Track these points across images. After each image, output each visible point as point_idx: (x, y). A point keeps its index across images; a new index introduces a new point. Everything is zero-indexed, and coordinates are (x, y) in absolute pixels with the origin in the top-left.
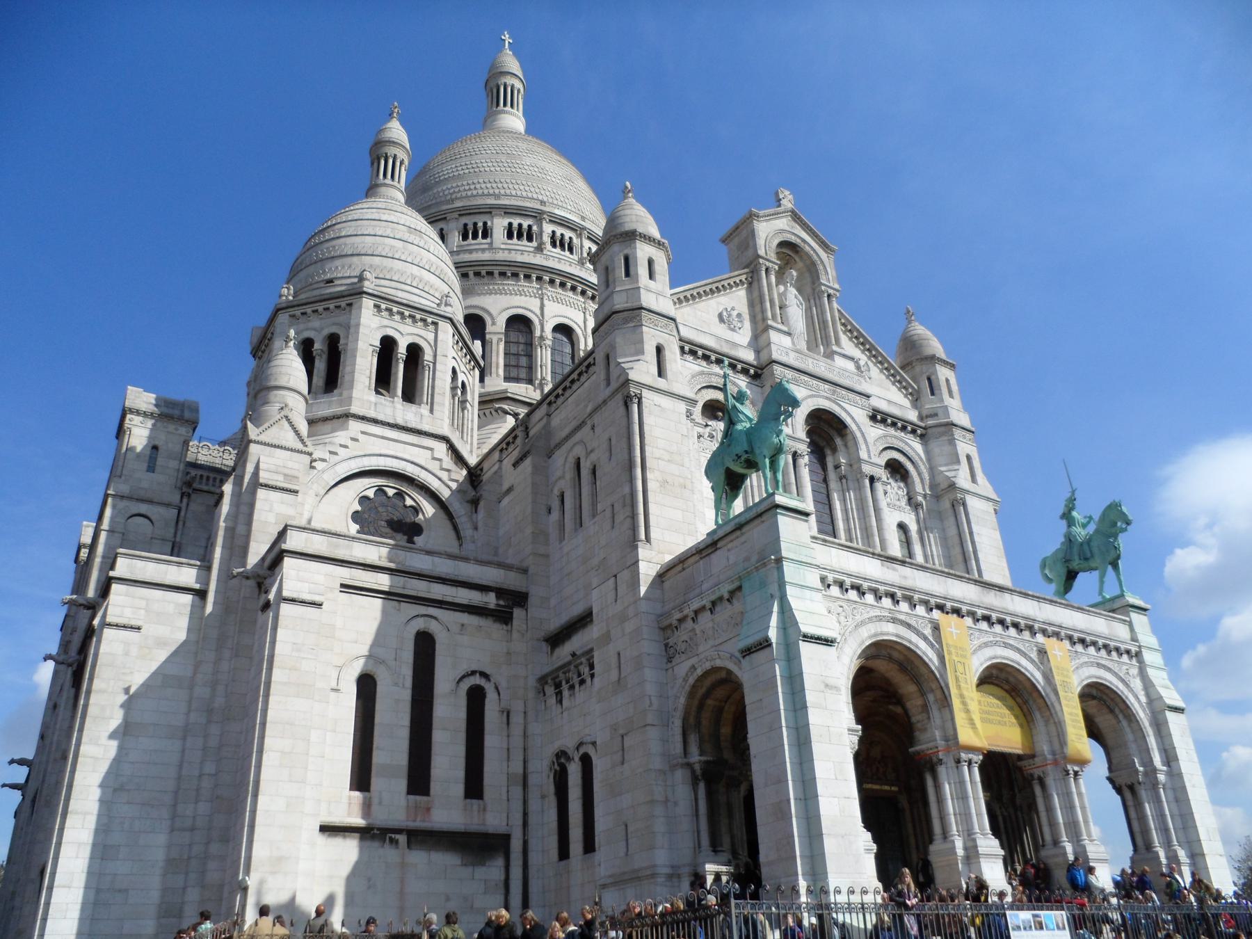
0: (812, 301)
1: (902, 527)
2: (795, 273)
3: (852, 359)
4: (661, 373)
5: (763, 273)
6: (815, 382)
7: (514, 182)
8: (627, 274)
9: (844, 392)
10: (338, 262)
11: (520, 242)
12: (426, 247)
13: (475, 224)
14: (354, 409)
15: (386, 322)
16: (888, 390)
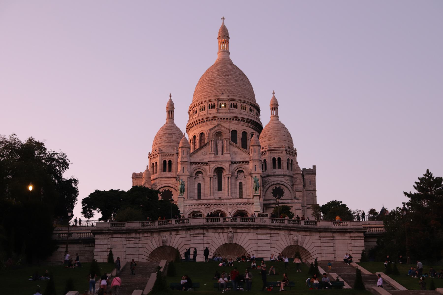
0: (224, 142)
1: (241, 183)
2: (219, 138)
3: (230, 153)
4: (183, 172)
5: (210, 142)
6: (217, 162)
7: (211, 90)
8: (180, 155)
9: (225, 162)
10: (156, 146)
11: (212, 109)
12: (172, 137)
13: (202, 106)
14: (160, 177)
15: (164, 158)
16: (242, 155)
